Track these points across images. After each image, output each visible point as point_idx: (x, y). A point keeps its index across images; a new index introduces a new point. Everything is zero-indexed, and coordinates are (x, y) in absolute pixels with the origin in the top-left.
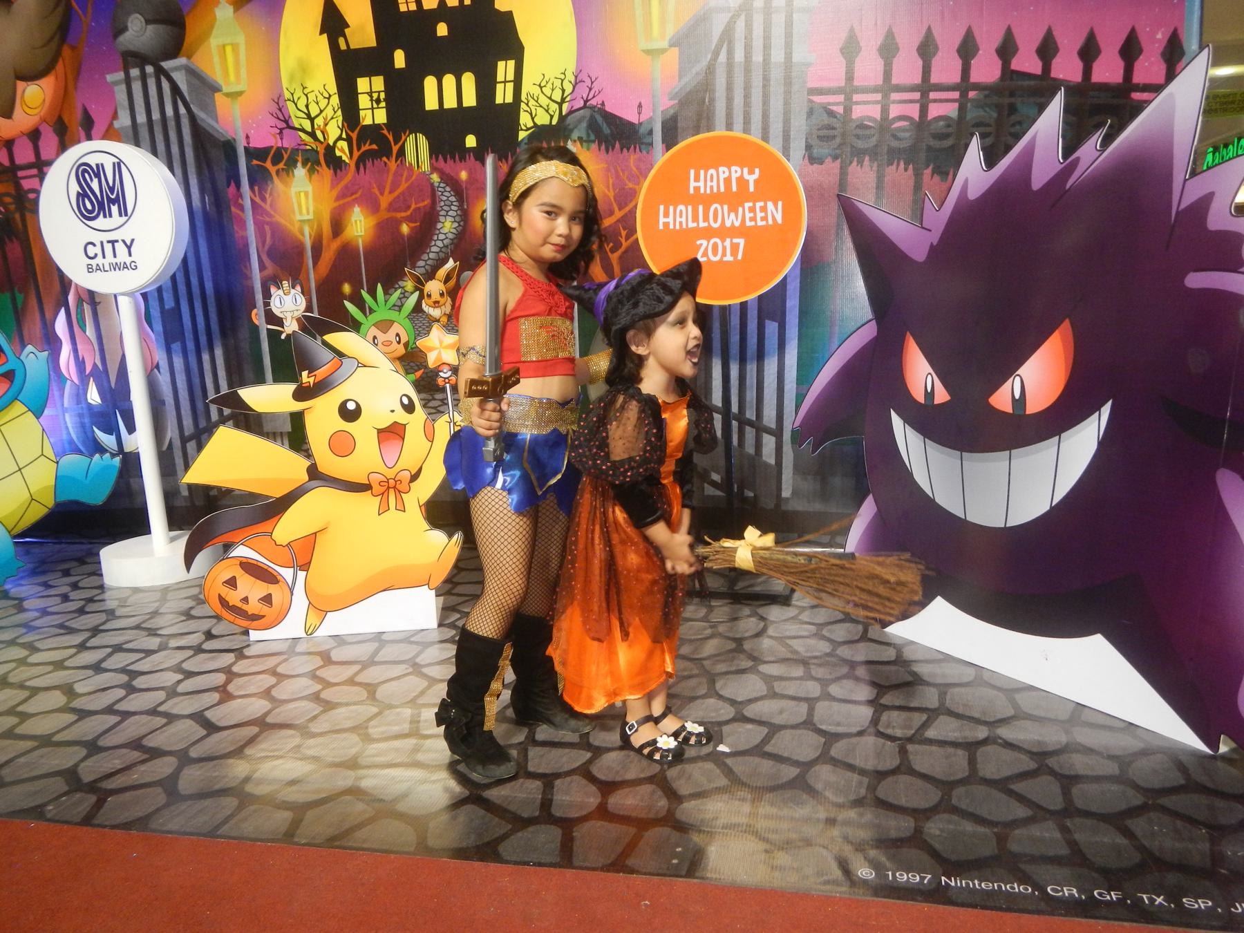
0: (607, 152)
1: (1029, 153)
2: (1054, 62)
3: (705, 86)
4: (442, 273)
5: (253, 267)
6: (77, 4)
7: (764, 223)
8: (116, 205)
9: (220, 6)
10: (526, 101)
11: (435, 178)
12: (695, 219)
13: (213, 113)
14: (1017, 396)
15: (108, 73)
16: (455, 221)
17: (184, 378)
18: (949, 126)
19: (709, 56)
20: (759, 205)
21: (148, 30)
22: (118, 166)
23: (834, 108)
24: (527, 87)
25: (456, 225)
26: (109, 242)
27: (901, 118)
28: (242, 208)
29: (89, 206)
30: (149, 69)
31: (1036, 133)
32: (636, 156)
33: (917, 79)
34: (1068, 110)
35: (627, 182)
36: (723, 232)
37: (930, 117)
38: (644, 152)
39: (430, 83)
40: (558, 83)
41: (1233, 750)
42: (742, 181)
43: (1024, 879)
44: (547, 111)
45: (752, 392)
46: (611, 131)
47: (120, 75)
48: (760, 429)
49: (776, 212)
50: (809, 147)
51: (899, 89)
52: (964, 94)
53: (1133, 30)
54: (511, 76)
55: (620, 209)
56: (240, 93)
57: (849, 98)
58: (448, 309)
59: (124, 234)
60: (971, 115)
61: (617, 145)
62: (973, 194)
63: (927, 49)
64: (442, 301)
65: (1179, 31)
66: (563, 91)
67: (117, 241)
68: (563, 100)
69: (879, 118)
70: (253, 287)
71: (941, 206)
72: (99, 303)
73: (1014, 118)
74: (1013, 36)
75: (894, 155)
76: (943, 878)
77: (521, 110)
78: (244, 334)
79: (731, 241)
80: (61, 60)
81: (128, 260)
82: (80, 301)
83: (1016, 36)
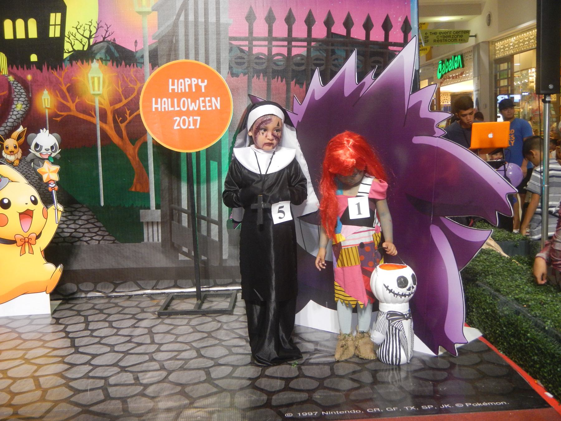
0: (117, 66)
1: (342, 78)
2: (352, 29)
3: (173, 33)
4: (16, 134)
7: (210, 109)
10: (68, 37)
11: (11, 78)
12: (173, 106)
16: (24, 104)
18: (302, 59)
19: (175, 17)
20: (207, 99)
23: (244, 48)
24: (69, 28)
25: (24, 106)
27: (278, 54)
31: (345, 69)
32: (135, 68)
33: (285, 35)
34: (359, 60)
35: (129, 84)
36: (189, 113)
37: (292, 55)
38: (139, 68)
39: (8, 24)
40: (87, 27)
41: (444, 353)
42: (198, 86)
43: (358, 408)
44: (81, 42)
45: (204, 200)
46: (120, 55)
48: (209, 221)
49: (216, 103)
50: (230, 68)
51: (277, 39)
52: (309, 44)
53: (388, 16)
54: (59, 22)
55: (125, 99)
57: (250, 43)
58: (19, 155)
60: (314, 54)
61: (123, 63)
62: (318, 97)
63: (289, 20)
64: (16, 151)
65: (409, 18)
66: (91, 32)
68: (90, 37)
69: (267, 54)
71: (302, 102)
73: (334, 57)
75: (276, 73)
76: (323, 412)
77: (65, 41)
79: (193, 118)
83: (333, 16)
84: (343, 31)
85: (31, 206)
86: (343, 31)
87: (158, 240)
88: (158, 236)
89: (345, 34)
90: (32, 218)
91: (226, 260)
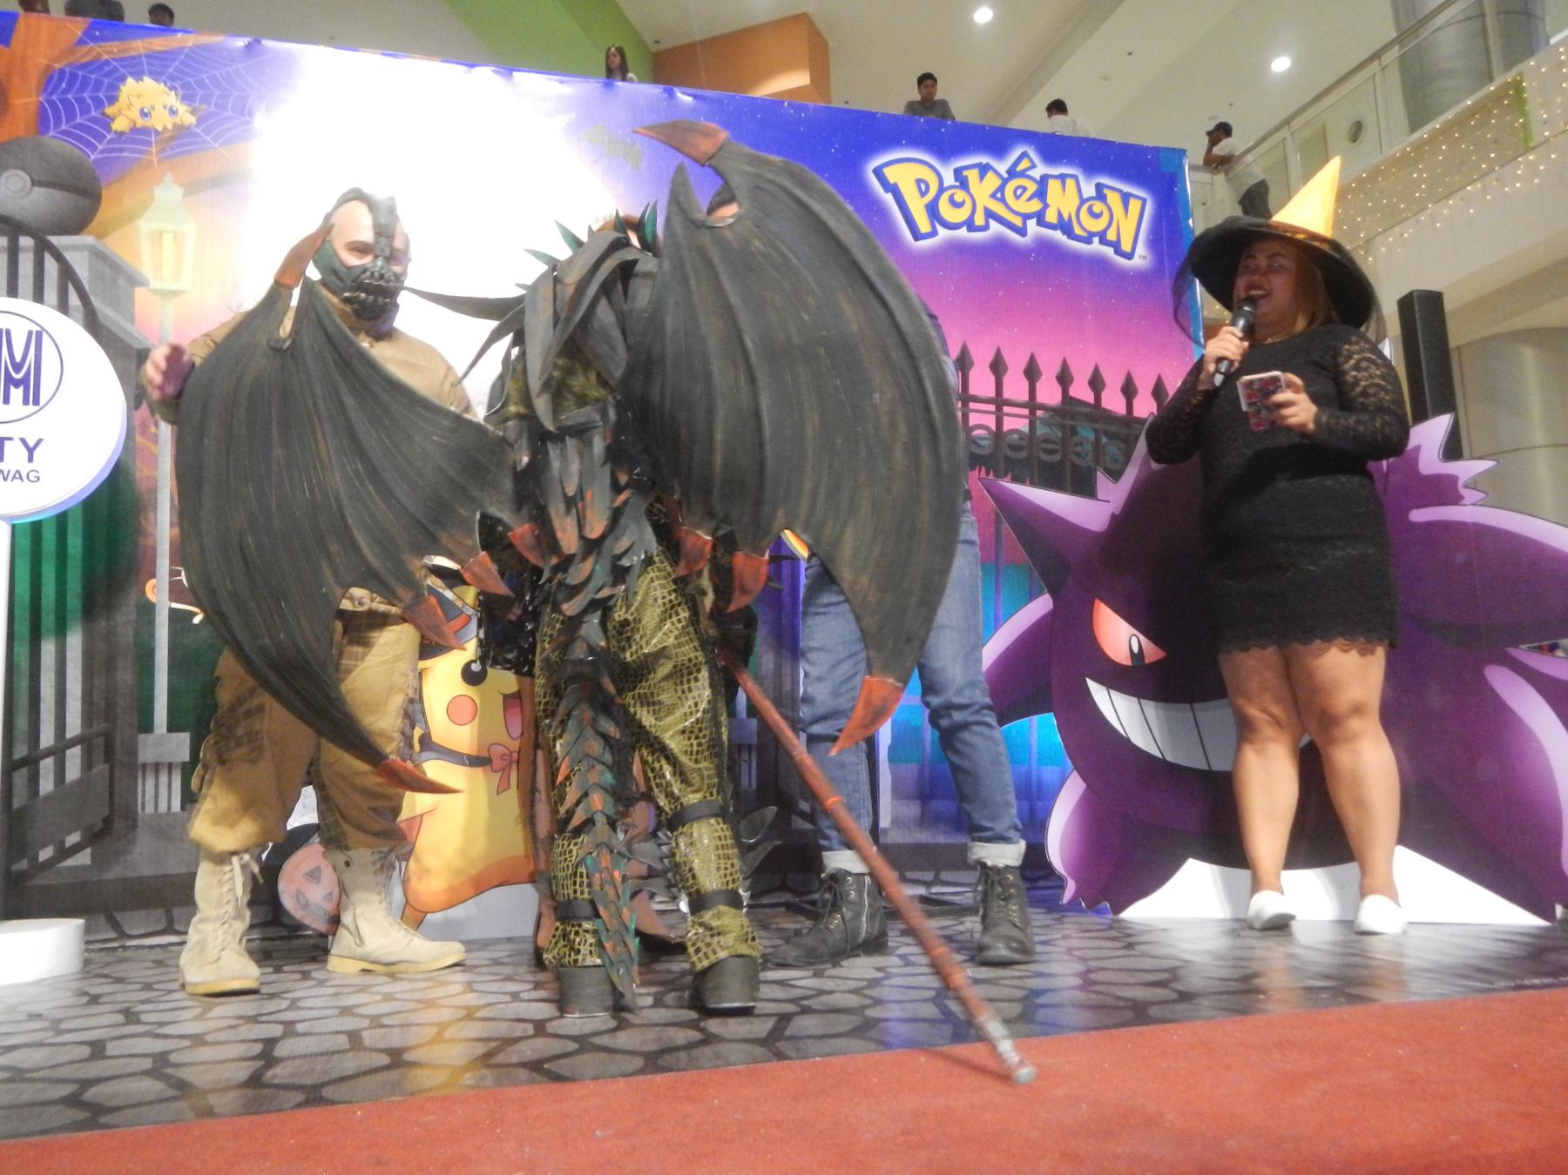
5: (159, 521)
8: (21, 388)
13: (128, 311)
18: (1021, 439)
22: (36, 338)
28: (155, 439)
30: (26, 242)
33: (992, 394)
52: (1032, 413)
56: (176, 293)
60: (1041, 431)
63: (998, 367)
67: (10, 439)
70: (154, 550)
73: (1075, 439)
74: (1068, 369)
78: (125, 617)
81: (25, 467)
84: (1089, 397)
86: (1089, 397)
87: (750, 785)
88: (750, 777)
89: (1092, 401)
91: (885, 830)
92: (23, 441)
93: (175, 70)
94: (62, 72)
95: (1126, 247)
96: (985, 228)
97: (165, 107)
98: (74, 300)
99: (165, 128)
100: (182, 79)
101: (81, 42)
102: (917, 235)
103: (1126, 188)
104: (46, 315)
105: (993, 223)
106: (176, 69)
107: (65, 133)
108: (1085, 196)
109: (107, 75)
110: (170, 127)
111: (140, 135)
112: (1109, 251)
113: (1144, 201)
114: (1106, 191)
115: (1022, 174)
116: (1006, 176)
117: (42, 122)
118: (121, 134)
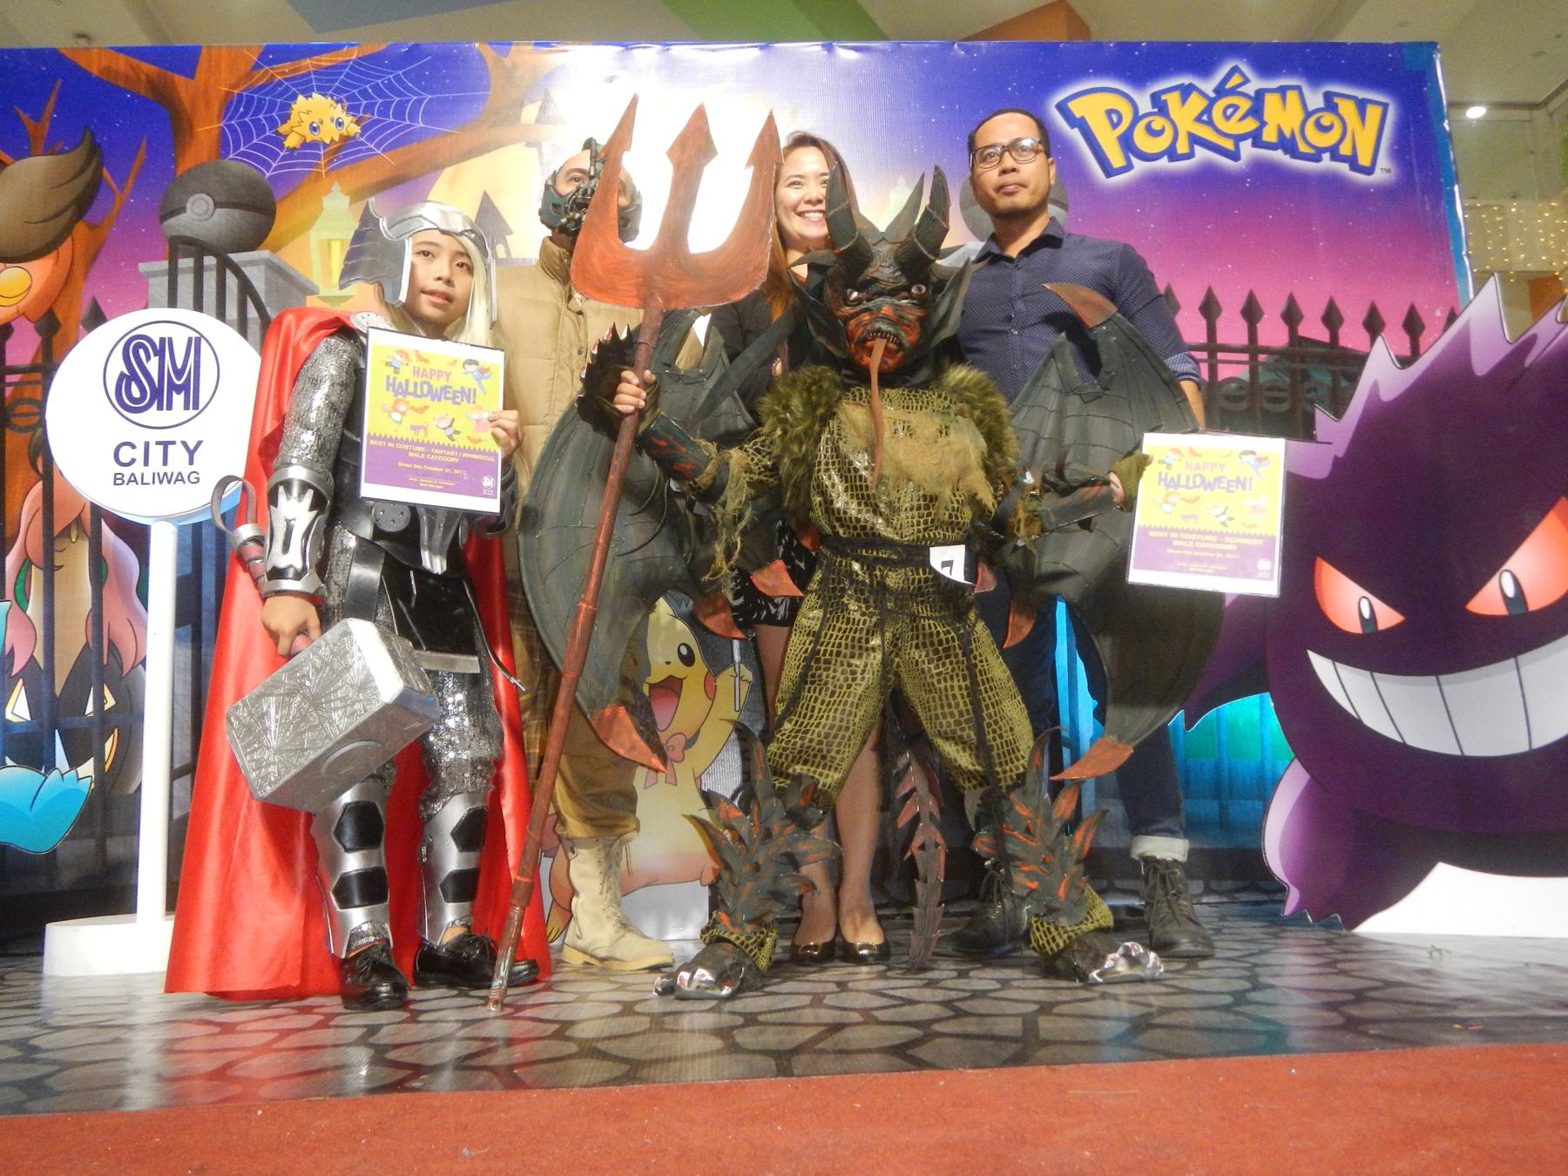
6: (111, 175)
8: (183, 394)
9: (331, 195)
14: (1510, 592)
15: (144, 260)
17: (189, 678)
18: (1241, 388)
21: (215, 216)
22: (195, 344)
26: (158, 443)
29: (136, 393)
33: (1203, 339)
37: (1220, 379)
47: (165, 265)
52: (1253, 357)
59: (190, 434)
60: (1265, 377)
62: (1388, 394)
67: (173, 443)
71: (1338, 409)
72: (61, 567)
73: (1307, 385)
80: (69, 240)
81: (186, 471)
82: (26, 563)
84: (1322, 334)
85: (678, 669)
86: (1322, 334)
90: (679, 696)
92: (184, 444)
93: (342, 82)
94: (240, 95)
95: (1364, 159)
96: (1190, 155)
97: (332, 120)
98: (252, 313)
99: (332, 140)
100: (347, 91)
101: (257, 67)
102: (1109, 171)
103: (1362, 94)
104: (205, 322)
105: (1197, 148)
106: (342, 82)
107: (244, 154)
108: (1311, 108)
109: (280, 95)
110: (337, 139)
111: (309, 149)
112: (1344, 168)
113: (1385, 106)
114: (1336, 100)
115: (1233, 92)
116: (1213, 95)
117: (223, 147)
118: (294, 149)
